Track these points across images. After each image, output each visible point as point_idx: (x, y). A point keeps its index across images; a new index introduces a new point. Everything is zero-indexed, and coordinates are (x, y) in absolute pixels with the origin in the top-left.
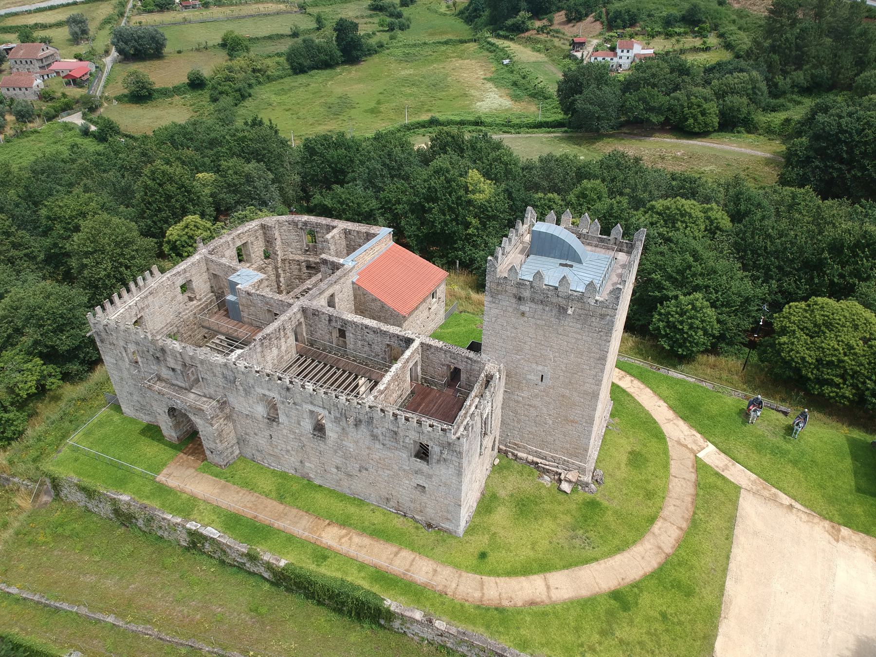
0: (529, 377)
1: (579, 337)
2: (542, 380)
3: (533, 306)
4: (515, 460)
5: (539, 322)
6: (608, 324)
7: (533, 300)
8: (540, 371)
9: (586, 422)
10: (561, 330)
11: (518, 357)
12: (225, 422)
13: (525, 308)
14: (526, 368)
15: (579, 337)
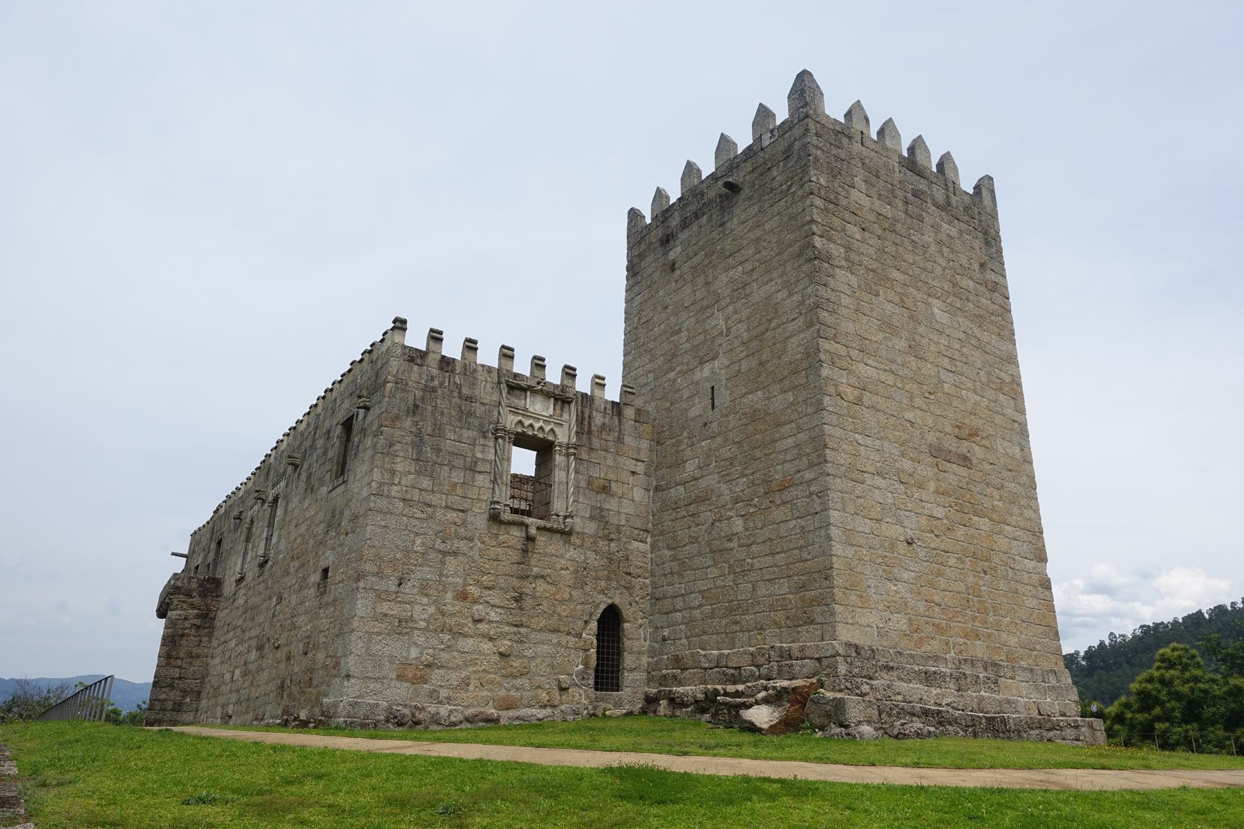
0: (693, 413)
1: (757, 233)
2: (713, 408)
3: (683, 236)
4: (673, 716)
5: (695, 261)
6: (799, 158)
7: (685, 225)
8: (708, 379)
9: (811, 466)
10: (728, 245)
11: (672, 375)
12: (197, 622)
13: (676, 252)
14: (686, 394)
15: (757, 233)
